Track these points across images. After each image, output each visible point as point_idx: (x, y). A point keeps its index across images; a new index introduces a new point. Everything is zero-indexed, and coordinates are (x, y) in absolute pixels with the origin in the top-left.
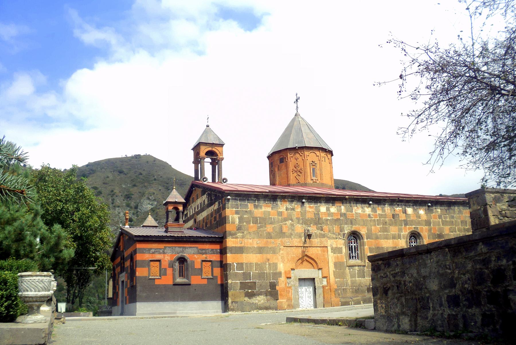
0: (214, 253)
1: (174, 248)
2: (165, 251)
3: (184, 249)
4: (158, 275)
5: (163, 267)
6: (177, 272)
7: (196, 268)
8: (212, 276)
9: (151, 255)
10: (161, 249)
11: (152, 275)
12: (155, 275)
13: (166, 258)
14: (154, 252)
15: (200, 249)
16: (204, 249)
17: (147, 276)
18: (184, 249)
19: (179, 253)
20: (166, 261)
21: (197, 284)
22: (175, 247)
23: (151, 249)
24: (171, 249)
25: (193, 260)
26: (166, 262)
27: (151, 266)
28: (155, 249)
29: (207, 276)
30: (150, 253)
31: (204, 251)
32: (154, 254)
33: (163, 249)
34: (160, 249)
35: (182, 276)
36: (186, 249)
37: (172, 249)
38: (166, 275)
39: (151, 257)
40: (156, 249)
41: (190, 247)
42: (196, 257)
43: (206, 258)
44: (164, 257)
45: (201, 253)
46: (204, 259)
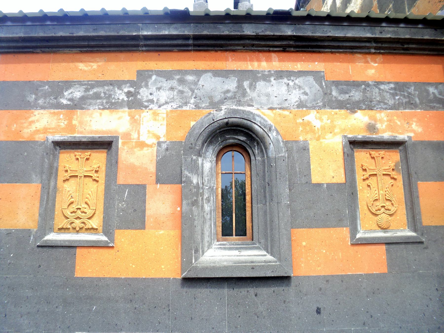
0: (411, 105)
1: (190, 78)
2: (144, 94)
3: (246, 84)
4: (95, 223)
5: (122, 179)
6: (207, 208)
7: (319, 185)
8: (415, 231)
9: (62, 114)
10: (119, 84)
11: (64, 223)
12: (78, 223)
13: (143, 130)
14: (83, 98)
15: (337, 83)
16: (356, 85)
17: (29, 231)
18: (246, 84)
19: (222, 102)
20: (142, 145)
21: (327, 279)
22: (199, 73)
23: (68, 84)
24: (174, 83)
25: (301, 138)
26: (146, 151)
27: (62, 175)
28: (90, 85)
29: (385, 229)
30: (59, 106)
31: (356, 95)
32: (79, 112)
33: (132, 83)
34: (111, 83)
35: (242, 232)
36: (261, 84)
37: (182, 81)
38: (143, 227)
39: (63, 124)
40: (93, 87)
41: (280, 75)
42: (317, 124)
43: (371, 128)
44: (135, 122)
45: (341, 105)
46: (360, 136)
